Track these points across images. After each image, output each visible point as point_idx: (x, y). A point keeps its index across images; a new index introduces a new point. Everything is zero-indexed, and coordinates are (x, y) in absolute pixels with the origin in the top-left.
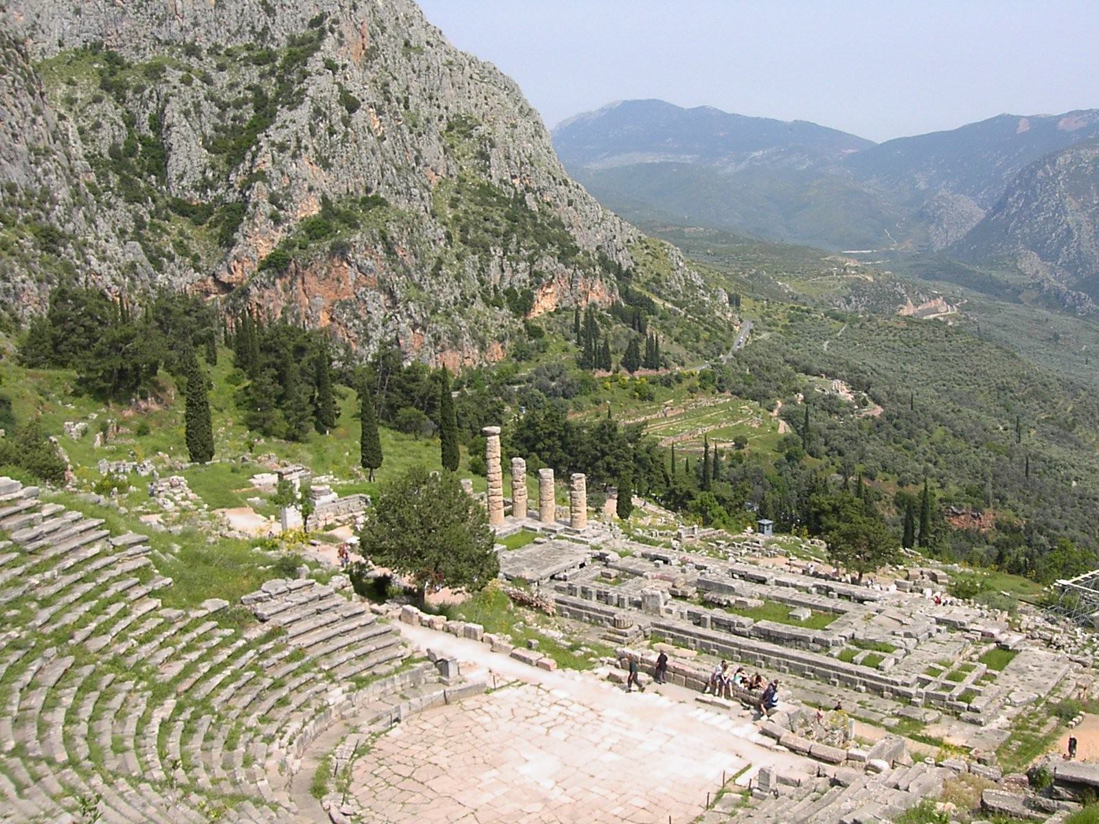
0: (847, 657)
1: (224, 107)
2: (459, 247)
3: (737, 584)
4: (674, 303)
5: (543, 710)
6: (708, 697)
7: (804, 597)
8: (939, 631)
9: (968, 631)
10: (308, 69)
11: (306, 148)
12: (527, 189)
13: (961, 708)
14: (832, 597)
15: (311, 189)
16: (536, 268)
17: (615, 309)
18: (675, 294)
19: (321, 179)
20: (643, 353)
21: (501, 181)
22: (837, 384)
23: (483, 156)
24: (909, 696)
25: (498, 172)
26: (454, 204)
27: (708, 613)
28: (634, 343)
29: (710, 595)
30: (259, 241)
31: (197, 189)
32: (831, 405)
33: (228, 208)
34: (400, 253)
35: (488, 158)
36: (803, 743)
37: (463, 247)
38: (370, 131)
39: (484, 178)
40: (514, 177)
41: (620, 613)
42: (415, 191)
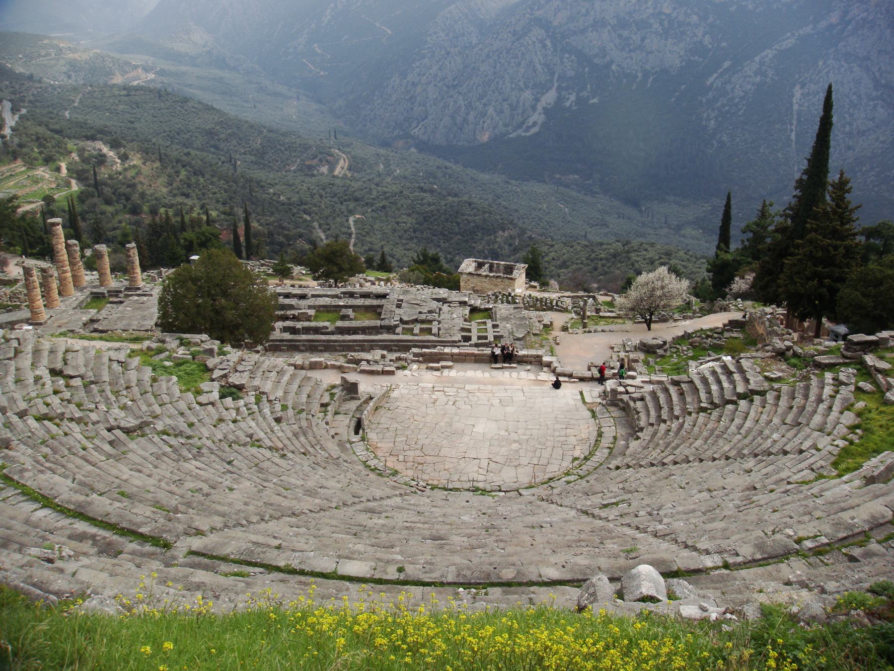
5: (434, 397)
14: (356, 298)
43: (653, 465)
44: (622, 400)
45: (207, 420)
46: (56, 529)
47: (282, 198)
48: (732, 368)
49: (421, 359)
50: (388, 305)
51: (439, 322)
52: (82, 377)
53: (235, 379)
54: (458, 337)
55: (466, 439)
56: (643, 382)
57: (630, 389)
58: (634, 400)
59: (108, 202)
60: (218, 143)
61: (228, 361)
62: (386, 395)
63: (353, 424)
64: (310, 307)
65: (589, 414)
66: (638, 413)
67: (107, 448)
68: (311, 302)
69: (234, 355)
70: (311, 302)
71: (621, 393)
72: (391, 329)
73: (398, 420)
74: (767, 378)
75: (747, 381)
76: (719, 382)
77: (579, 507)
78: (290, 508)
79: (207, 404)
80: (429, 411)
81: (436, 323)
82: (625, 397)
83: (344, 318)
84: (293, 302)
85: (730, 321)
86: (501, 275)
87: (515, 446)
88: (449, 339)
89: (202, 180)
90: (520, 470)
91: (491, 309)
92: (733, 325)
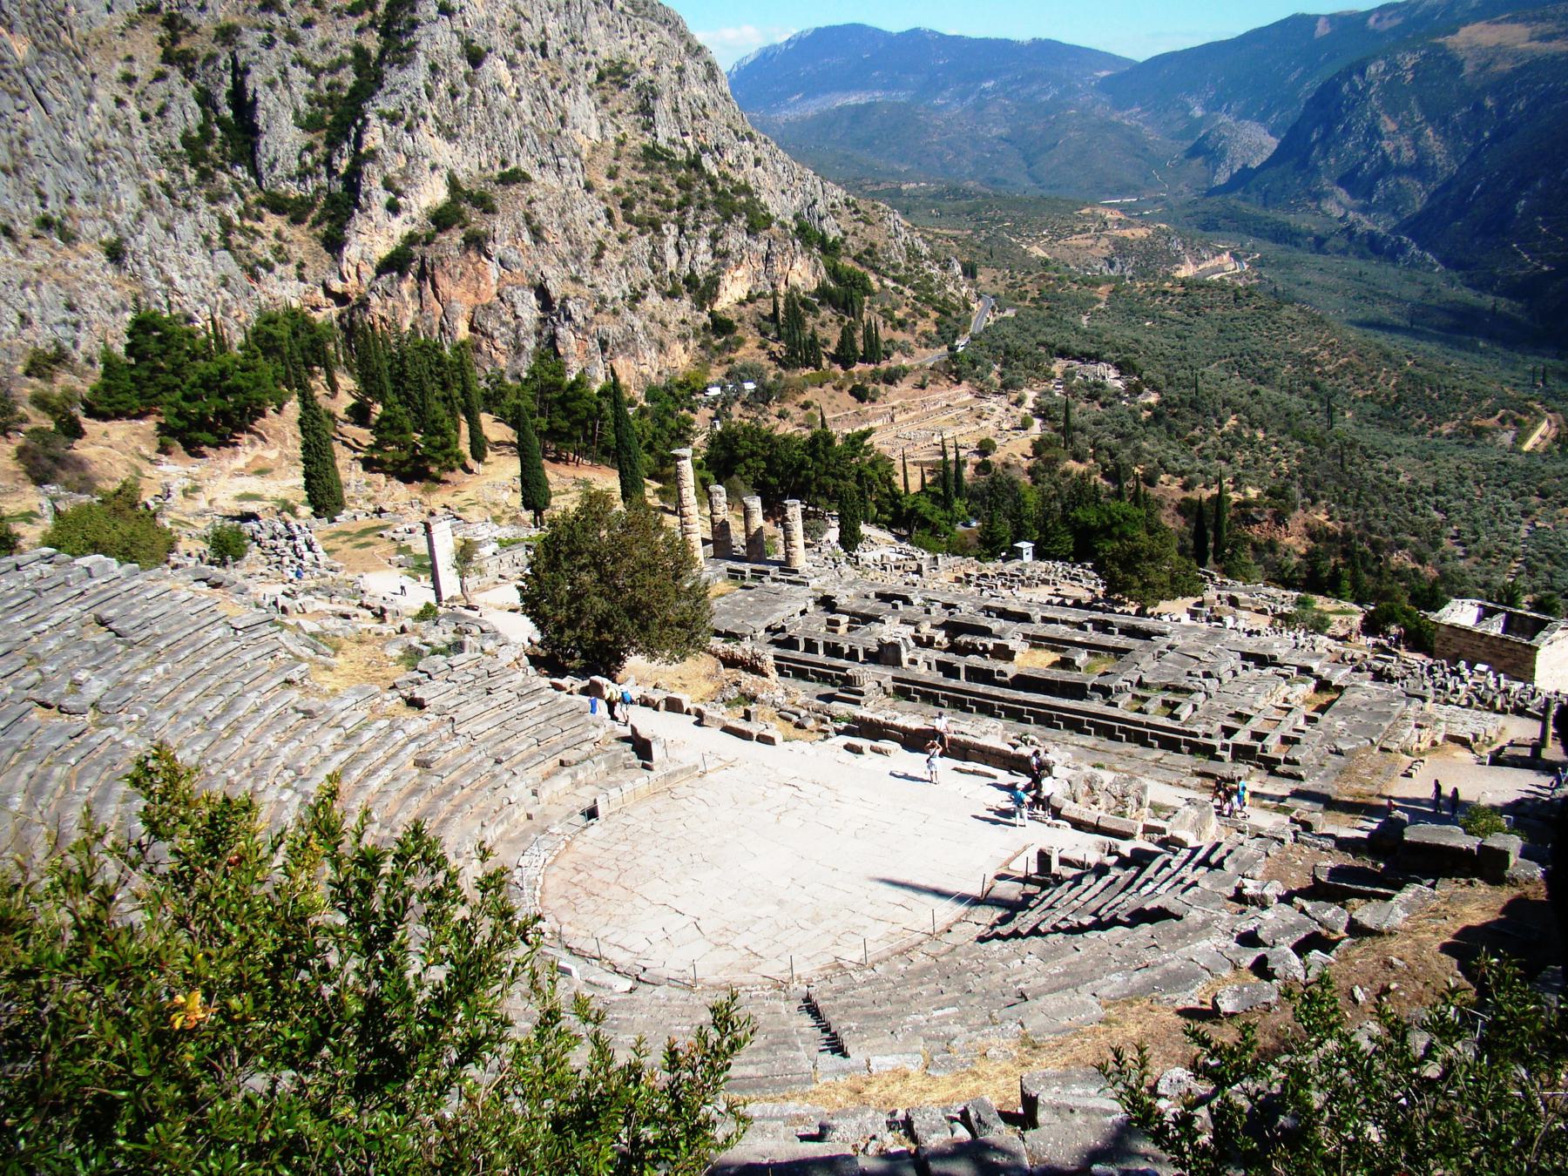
1: (317, 72)
2: (624, 228)
3: (996, 625)
4: (895, 280)
5: (770, 793)
6: (970, 766)
8: (1245, 668)
10: (416, 16)
11: (424, 117)
12: (703, 149)
13: (1278, 761)
14: (1112, 633)
15: (434, 168)
16: (719, 246)
17: (823, 293)
18: (895, 268)
19: (443, 151)
20: (860, 346)
21: (672, 142)
22: (1101, 368)
23: (646, 110)
24: (1214, 747)
25: (665, 132)
26: (612, 176)
27: (961, 662)
28: (847, 335)
29: (964, 639)
30: (373, 237)
31: (292, 179)
33: (332, 200)
34: (551, 240)
35: (651, 113)
36: (1090, 815)
37: (628, 227)
38: (501, 89)
39: (647, 139)
40: (685, 134)
41: (854, 669)
42: (564, 161)
47: (1401, 479)
59: (1079, 458)
60: (1319, 378)
64: (1026, 636)
70: (1029, 629)
83: (1066, 664)
86: (1512, 638)
89: (1260, 435)
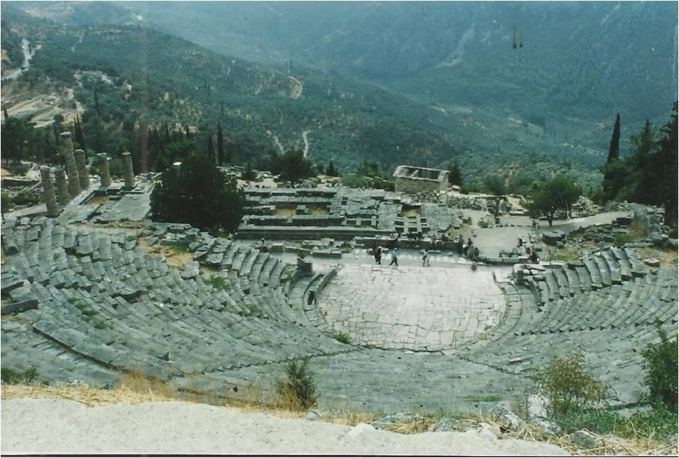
0: (353, 224)
5: (373, 275)
7: (293, 199)
9: (386, 201)
14: (309, 196)
27: (262, 218)
32: (101, 88)
43: (552, 332)
44: (527, 280)
45: (191, 291)
46: (75, 368)
47: (248, 116)
48: (618, 256)
49: (362, 245)
50: (335, 203)
51: (378, 217)
52: (91, 255)
53: (212, 259)
54: (392, 229)
55: (399, 309)
56: (544, 266)
57: (534, 272)
58: (537, 280)
59: (107, 120)
61: (207, 244)
62: (333, 274)
63: (307, 296)
64: (271, 204)
65: (501, 292)
66: (540, 290)
67: (112, 310)
68: (271, 199)
69: (209, 240)
70: (271, 199)
71: (527, 274)
72: (337, 222)
73: (344, 293)
74: (647, 263)
75: (631, 266)
76: (608, 267)
77: (490, 364)
78: (257, 359)
79: (190, 278)
80: (369, 287)
81: (374, 217)
82: (530, 278)
83: (299, 212)
84: (257, 199)
85: (618, 219)
86: (428, 179)
87: (440, 316)
88: (385, 230)
90: (442, 334)
91: (420, 206)
92: (621, 222)
